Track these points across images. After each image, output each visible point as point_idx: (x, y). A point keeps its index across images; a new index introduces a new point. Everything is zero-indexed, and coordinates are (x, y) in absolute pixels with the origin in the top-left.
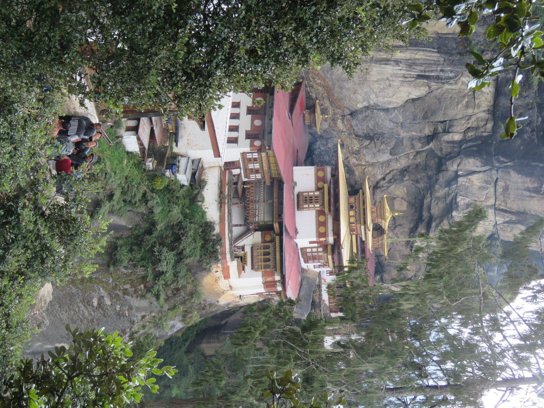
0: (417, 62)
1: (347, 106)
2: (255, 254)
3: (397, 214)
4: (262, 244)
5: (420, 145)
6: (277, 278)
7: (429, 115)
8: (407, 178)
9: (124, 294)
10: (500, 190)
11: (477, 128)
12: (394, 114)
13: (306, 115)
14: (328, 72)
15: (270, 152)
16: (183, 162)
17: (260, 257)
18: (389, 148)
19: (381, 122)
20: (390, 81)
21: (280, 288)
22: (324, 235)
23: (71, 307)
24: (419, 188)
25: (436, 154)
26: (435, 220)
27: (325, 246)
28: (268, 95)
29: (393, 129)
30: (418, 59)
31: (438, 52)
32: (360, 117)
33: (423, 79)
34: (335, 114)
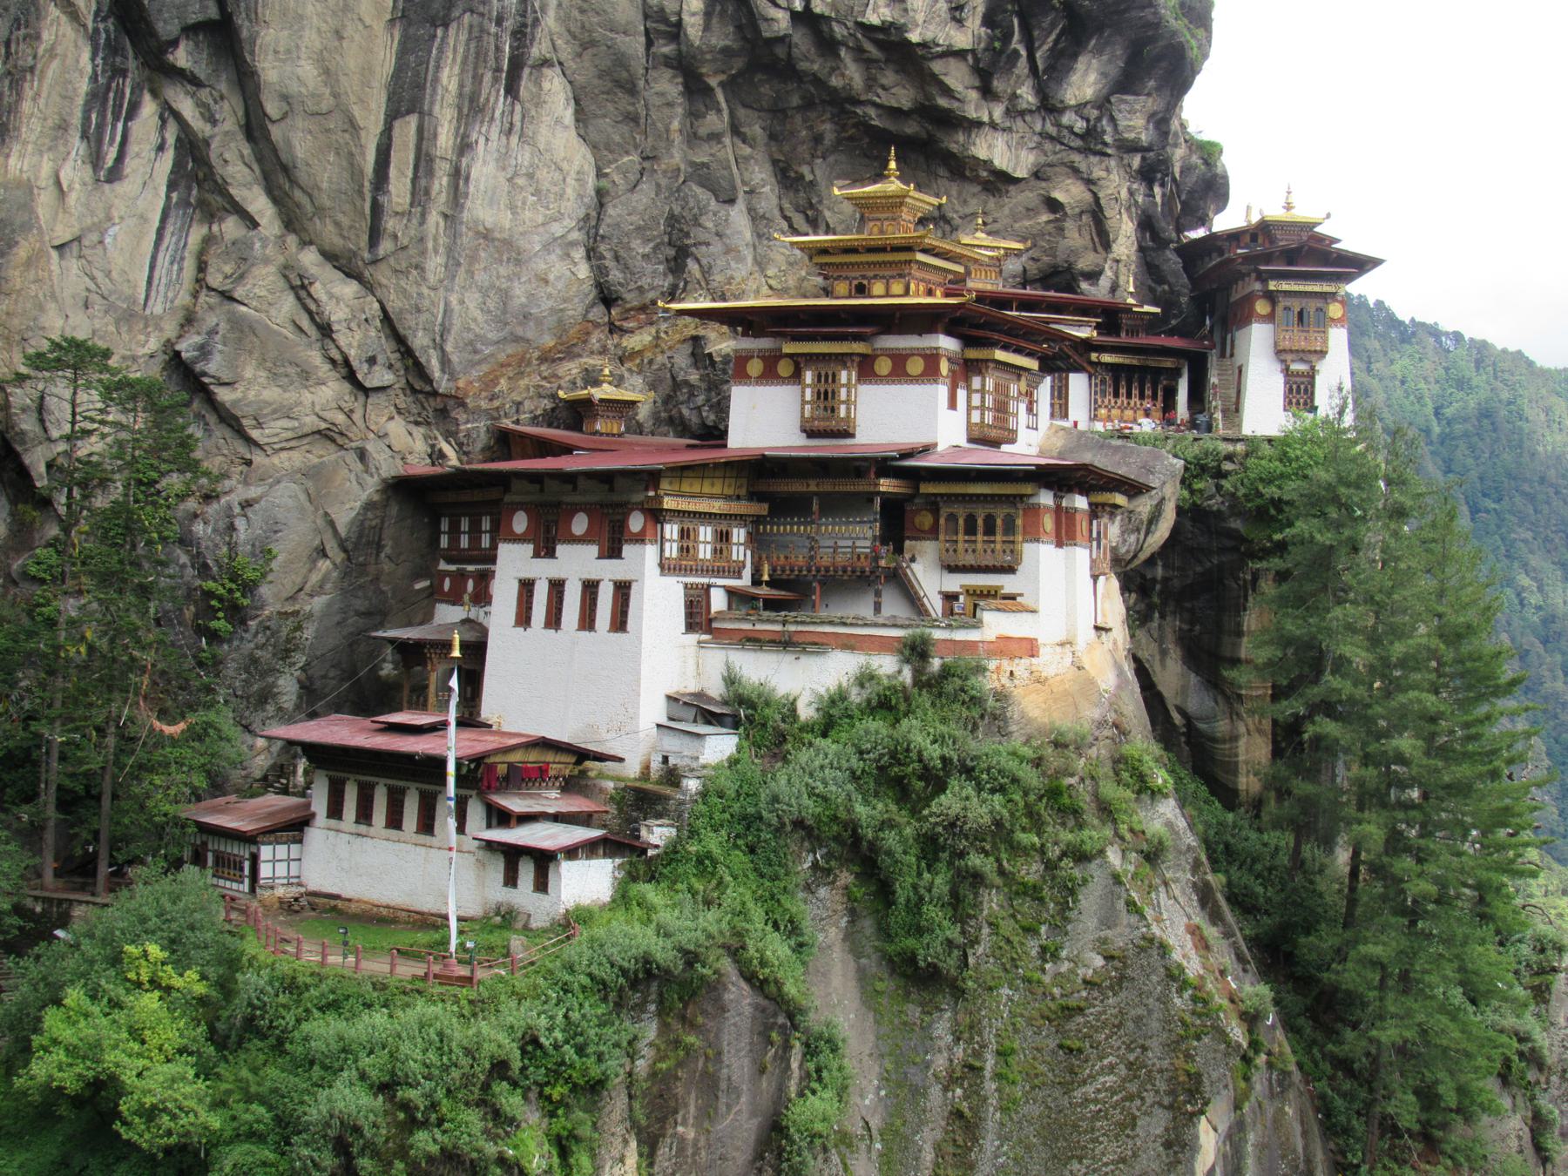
0: (467, 90)
1: (580, 309)
2: (969, 559)
3: (893, 165)
4: (942, 537)
5: (712, 117)
6: (1046, 498)
7: (625, 75)
8: (805, 170)
9: (1055, 957)
12: (617, 178)
13: (598, 427)
14: (476, 352)
15: (665, 485)
17: (979, 546)
18: (713, 202)
19: (634, 218)
20: (516, 174)
21: (1081, 502)
22: (931, 360)
23: (1084, 1124)
24: (839, 141)
25: (740, 73)
26: (929, 97)
27: (967, 369)
28: (507, 498)
29: (658, 185)
30: (461, 86)
31: (446, 26)
32: (615, 275)
33: (519, 77)
34: (603, 351)
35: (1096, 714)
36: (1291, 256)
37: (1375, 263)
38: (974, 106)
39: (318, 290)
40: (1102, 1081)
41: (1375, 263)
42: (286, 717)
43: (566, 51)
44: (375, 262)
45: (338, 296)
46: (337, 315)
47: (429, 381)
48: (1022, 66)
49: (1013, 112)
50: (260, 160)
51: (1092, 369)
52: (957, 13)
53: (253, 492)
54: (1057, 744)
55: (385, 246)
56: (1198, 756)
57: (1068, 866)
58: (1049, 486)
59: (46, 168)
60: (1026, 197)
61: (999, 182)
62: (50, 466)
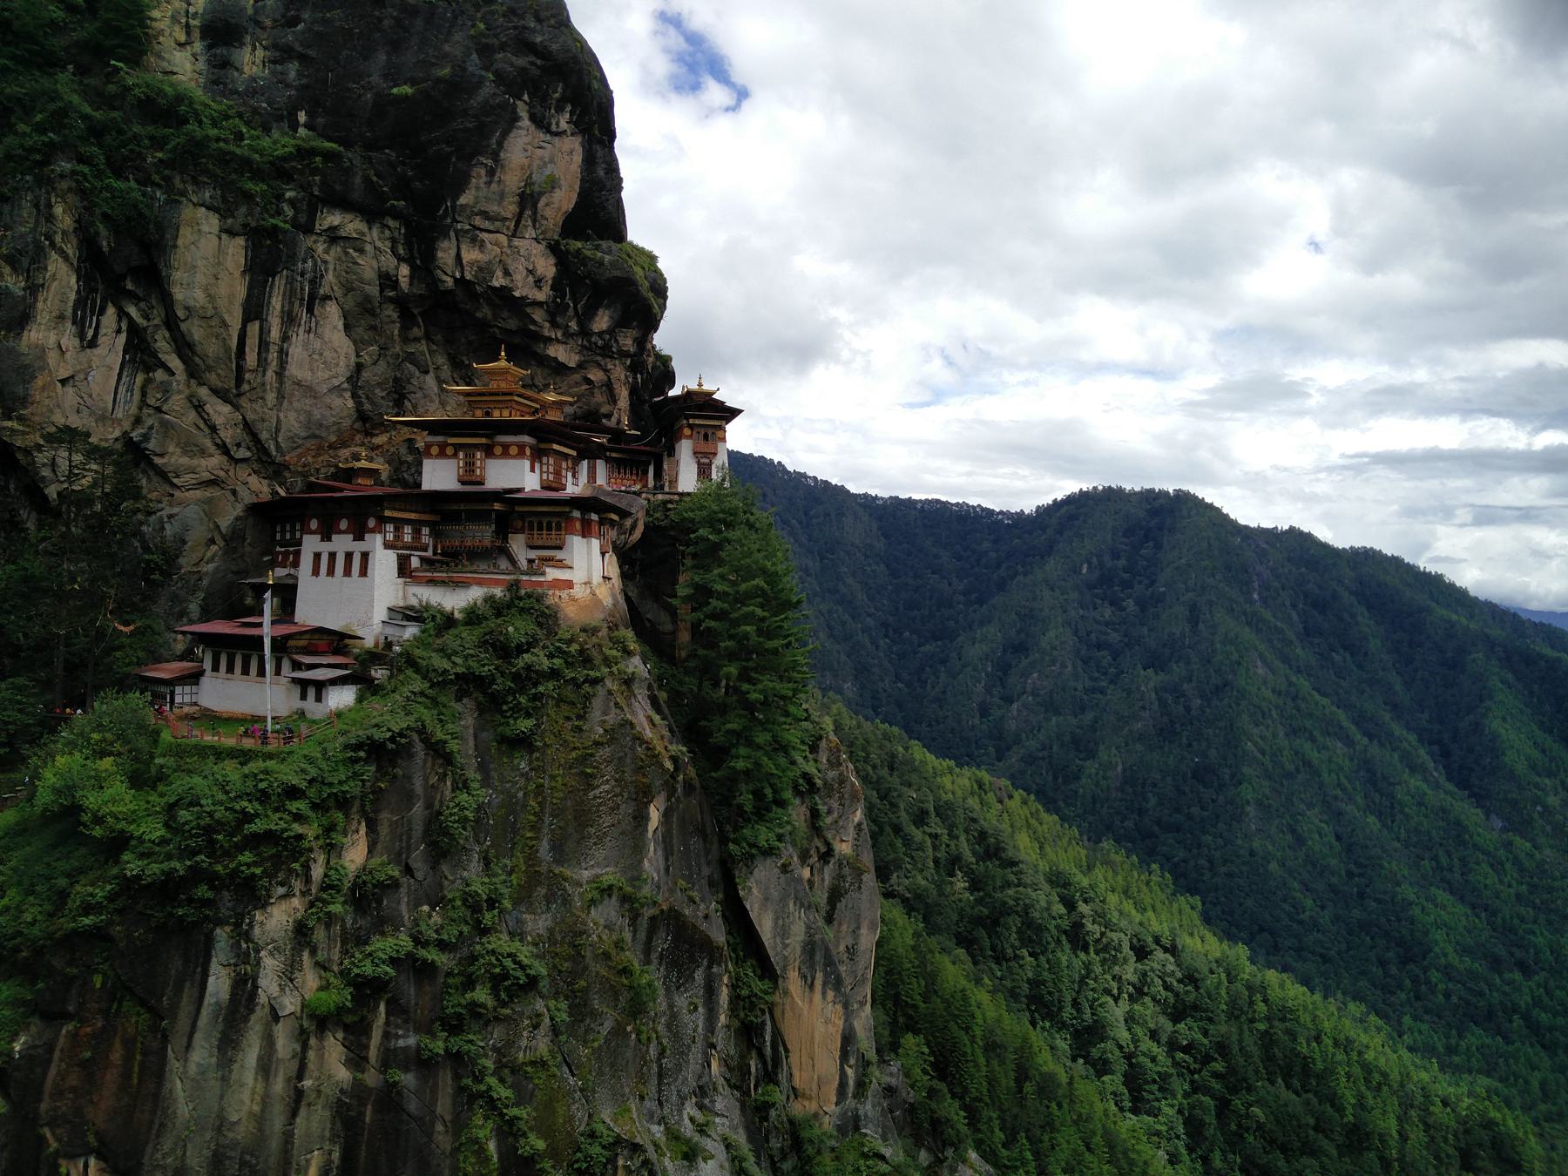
2: (540, 543)
5: (415, 329)
6: (576, 514)
10: (487, 225)
11: (394, 241)
16: (389, 631)
21: (594, 517)
22: (521, 447)
32: (367, 406)
34: (363, 444)
35: (602, 616)
36: (701, 407)
37: (740, 411)
38: (547, 331)
39: (208, 408)
40: (604, 788)
41: (740, 411)
42: (191, 622)
43: (338, 292)
44: (239, 395)
45: (220, 412)
46: (219, 421)
47: (270, 456)
48: (571, 312)
49: (568, 335)
50: (175, 340)
51: (608, 460)
52: (538, 283)
53: (176, 510)
54: (584, 630)
55: (246, 387)
56: (656, 643)
57: (587, 688)
58: (578, 509)
59: (52, 339)
60: (577, 377)
61: (559, 369)
62: (59, 494)
